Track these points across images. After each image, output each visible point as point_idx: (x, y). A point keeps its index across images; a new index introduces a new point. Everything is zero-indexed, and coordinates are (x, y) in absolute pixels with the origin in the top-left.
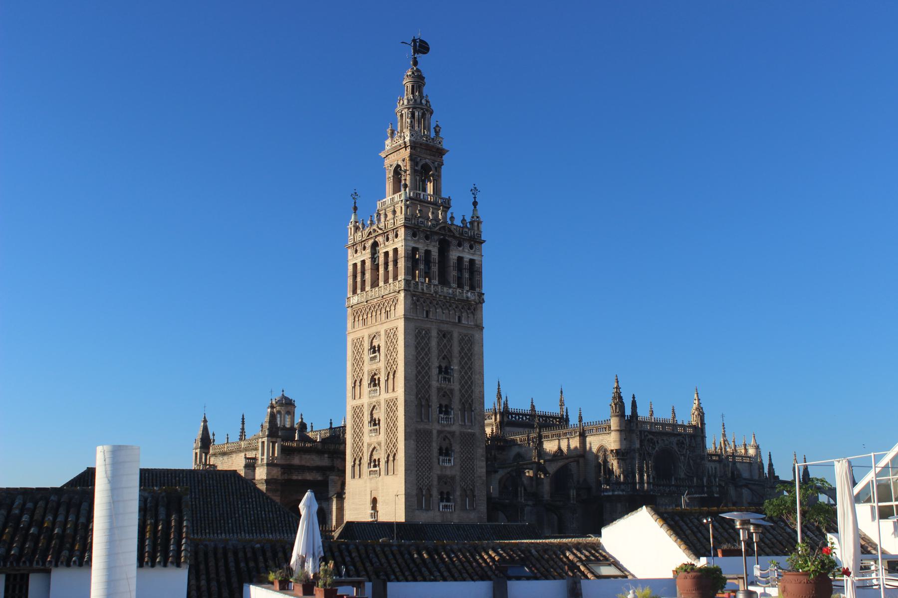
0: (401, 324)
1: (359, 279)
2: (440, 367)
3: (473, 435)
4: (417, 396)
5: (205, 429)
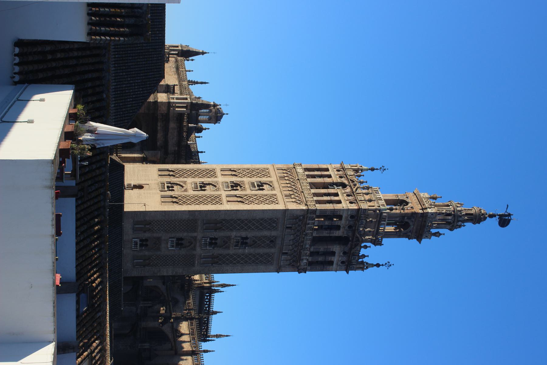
2: (247, 238)
3: (193, 265)
4: (224, 220)
5: (197, 53)
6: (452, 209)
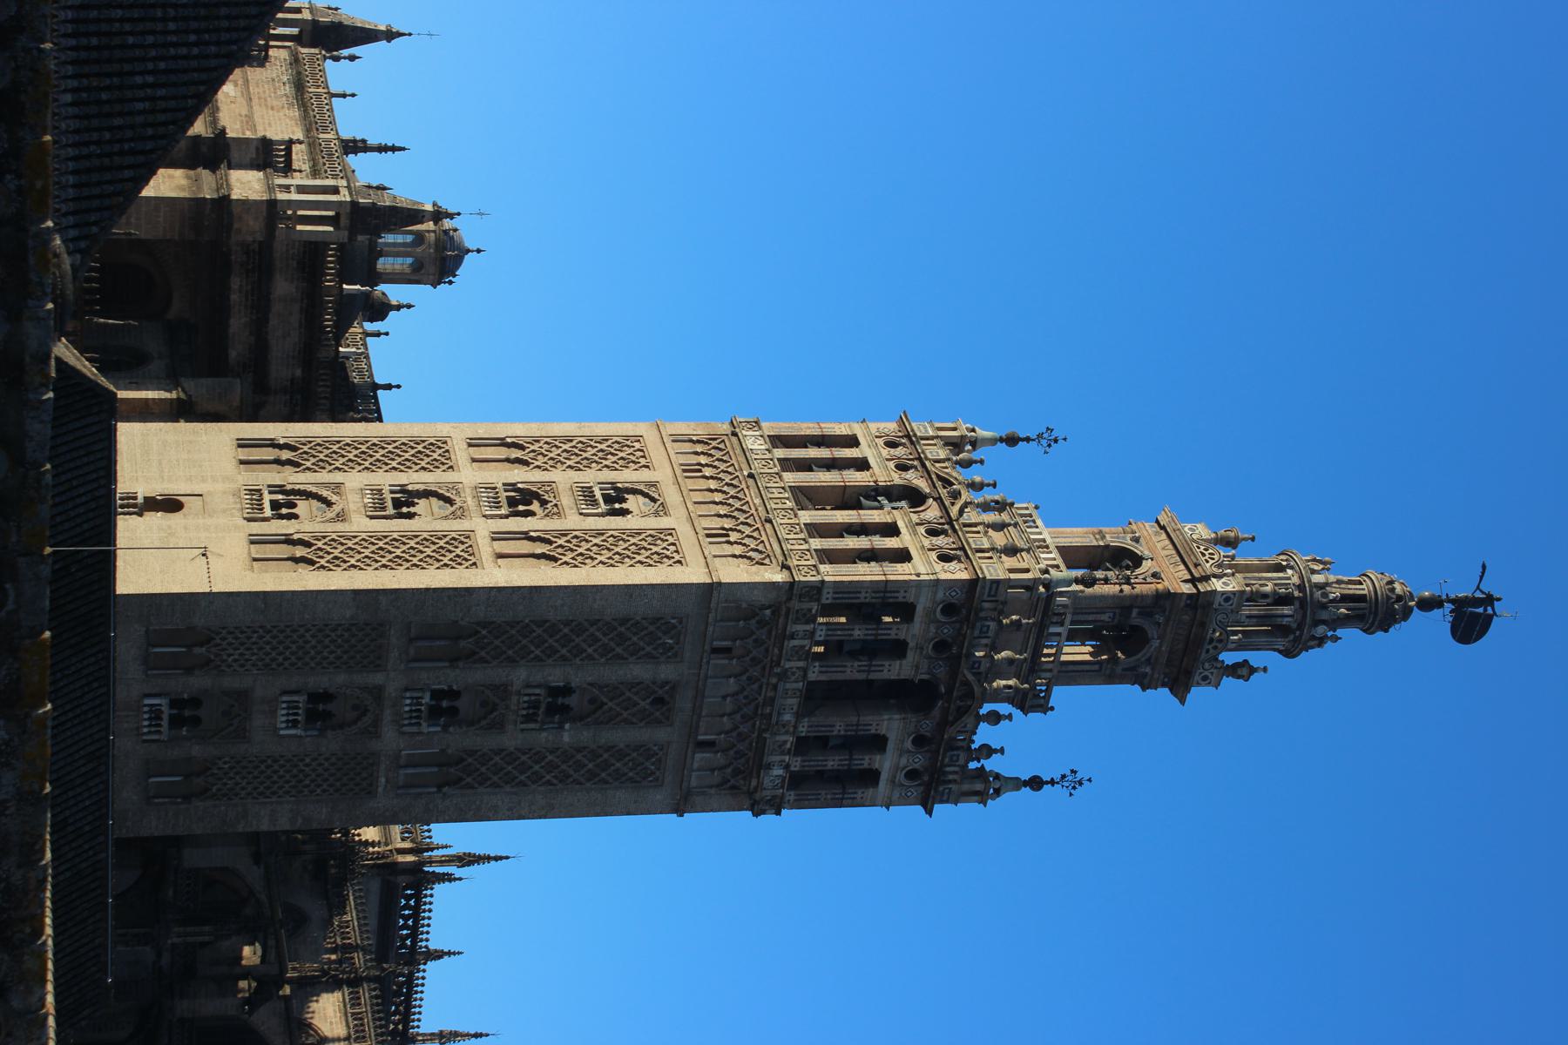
0: (691, 574)
1: (813, 453)
2: (566, 690)
3: (371, 793)
4: (485, 624)
5: (367, 36)
6: (1296, 580)
